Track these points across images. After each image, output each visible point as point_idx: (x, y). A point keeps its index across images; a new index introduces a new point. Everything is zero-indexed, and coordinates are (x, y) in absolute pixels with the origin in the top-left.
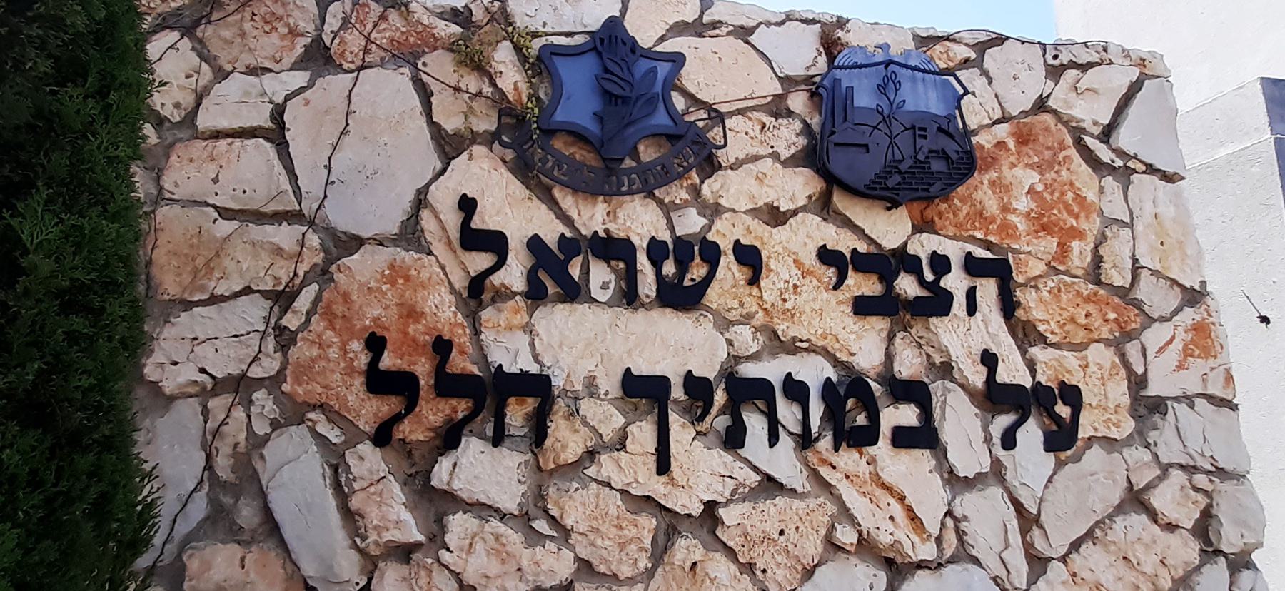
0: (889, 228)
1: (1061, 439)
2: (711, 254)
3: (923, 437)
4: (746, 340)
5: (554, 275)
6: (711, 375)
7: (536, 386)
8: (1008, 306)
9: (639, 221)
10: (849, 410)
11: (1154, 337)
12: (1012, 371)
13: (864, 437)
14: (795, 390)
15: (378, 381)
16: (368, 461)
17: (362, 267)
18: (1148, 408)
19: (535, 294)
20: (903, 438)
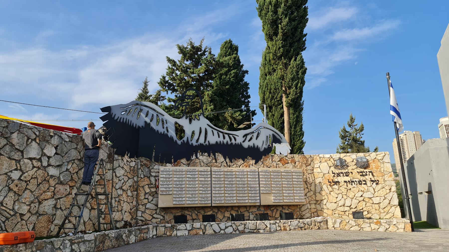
0: (362, 170)
1: (377, 184)
2: (349, 173)
3: (366, 184)
4: (352, 178)
5: (338, 175)
6: (349, 180)
7: (338, 182)
8: (372, 174)
9: (343, 171)
10: (360, 182)
11: (386, 176)
12: (373, 179)
13: (361, 184)
14: (356, 181)
15: (329, 182)
16: (329, 186)
17: (326, 175)
18: (384, 181)
19: (337, 176)
20: (364, 184)
